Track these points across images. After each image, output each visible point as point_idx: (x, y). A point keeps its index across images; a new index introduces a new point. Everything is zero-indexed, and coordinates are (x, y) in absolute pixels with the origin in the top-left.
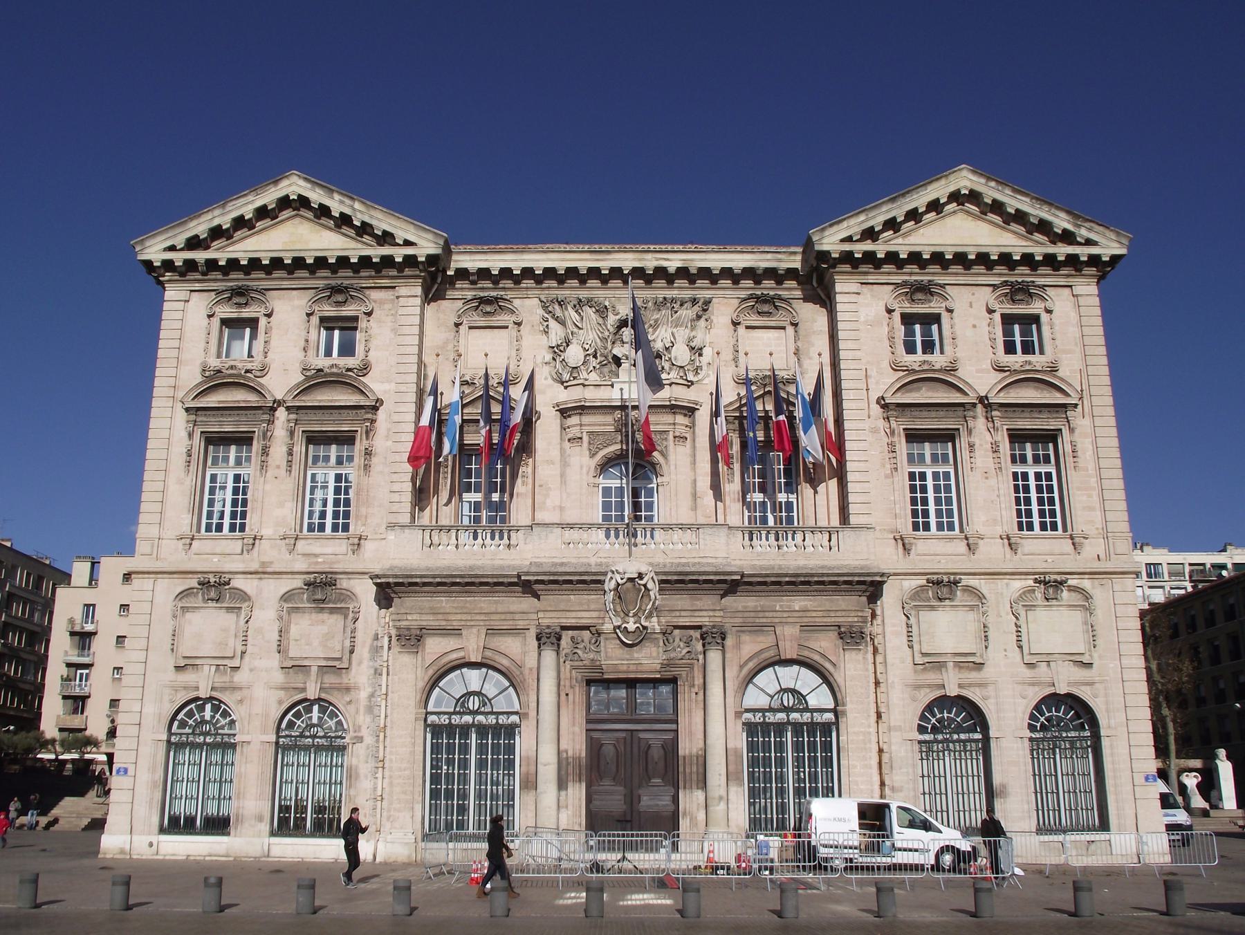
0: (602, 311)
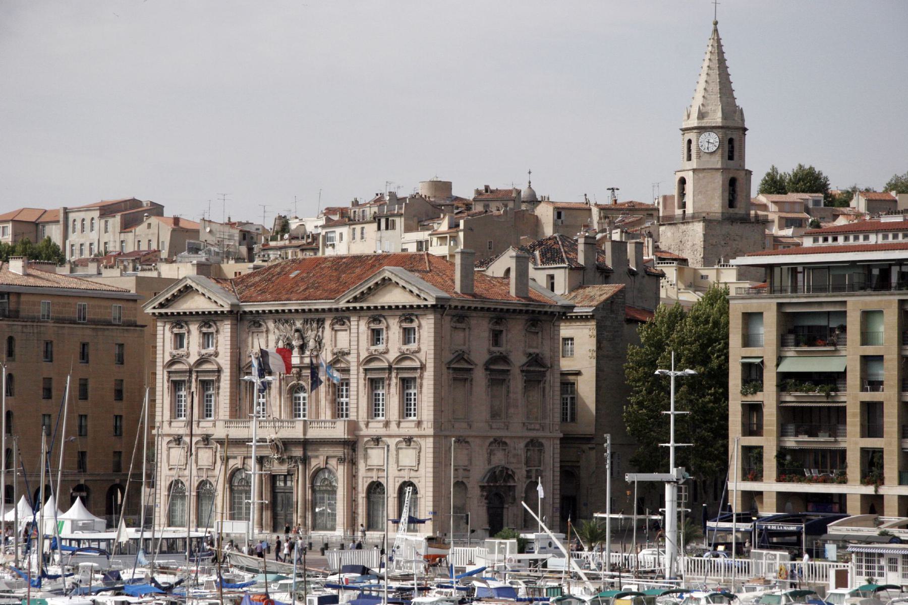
0: (291, 326)
